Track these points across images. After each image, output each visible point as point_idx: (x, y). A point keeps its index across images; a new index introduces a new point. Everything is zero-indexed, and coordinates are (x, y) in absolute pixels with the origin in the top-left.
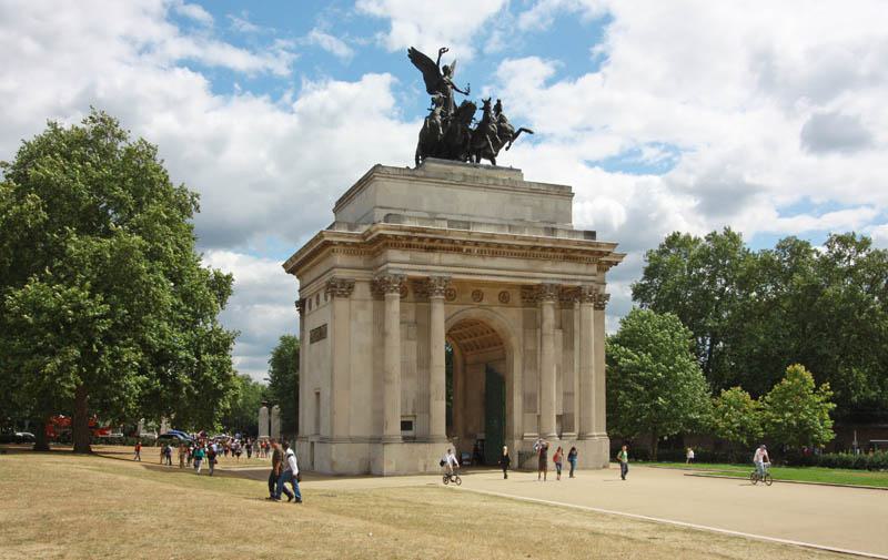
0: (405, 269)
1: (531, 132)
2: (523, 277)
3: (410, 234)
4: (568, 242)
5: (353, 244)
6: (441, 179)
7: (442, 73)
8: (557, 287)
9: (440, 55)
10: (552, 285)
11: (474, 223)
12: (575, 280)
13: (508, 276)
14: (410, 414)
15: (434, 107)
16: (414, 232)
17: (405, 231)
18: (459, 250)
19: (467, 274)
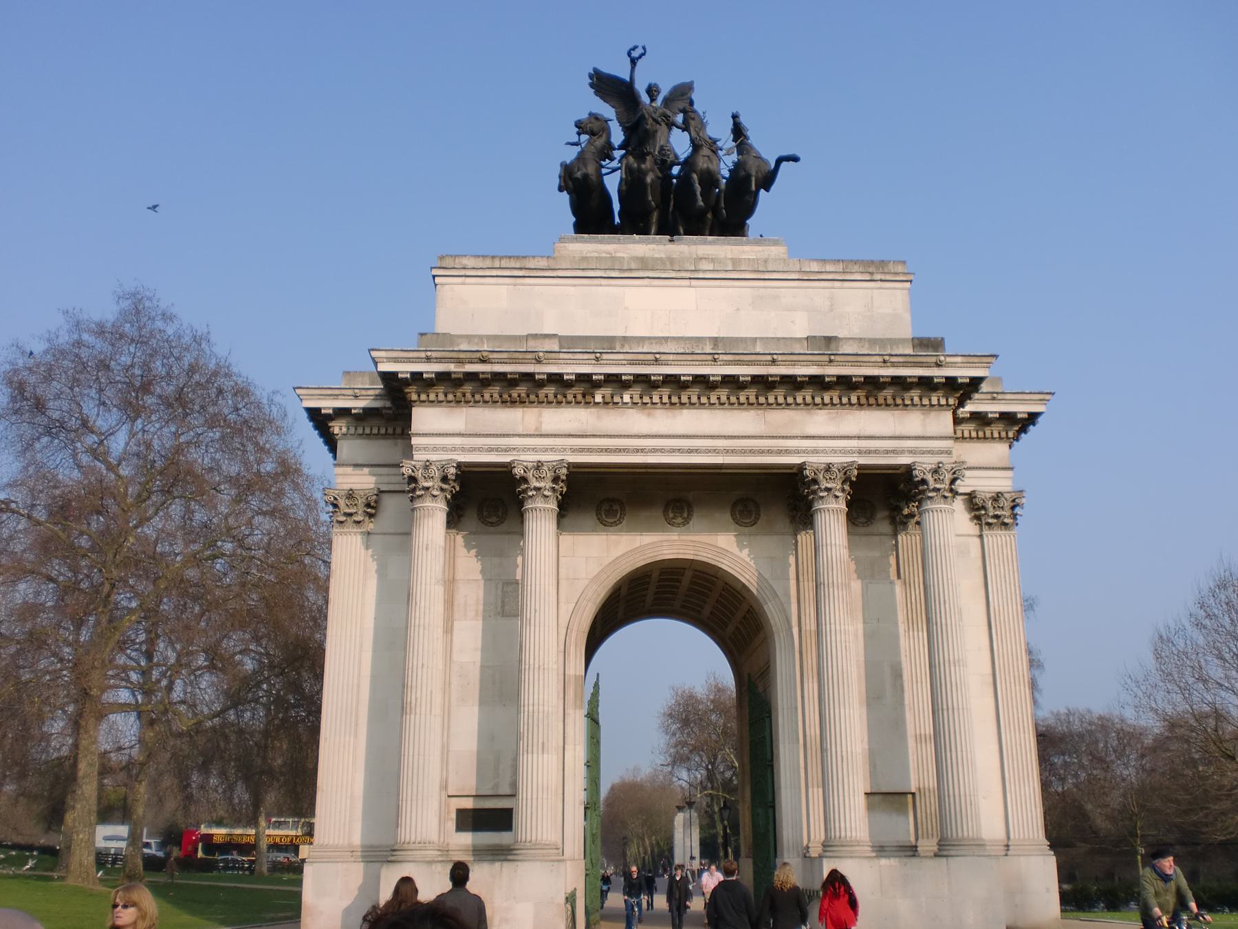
0: (454, 449)
1: (795, 159)
2: (752, 452)
3: (452, 367)
4: (856, 359)
5: (368, 413)
6: (583, 272)
7: (645, 98)
8: (845, 470)
9: (634, 62)
10: (828, 468)
11: (625, 338)
12: (894, 452)
13: (715, 451)
14: (508, 791)
15: (585, 137)
16: (460, 361)
17: (440, 360)
18: (586, 401)
19: (607, 451)
